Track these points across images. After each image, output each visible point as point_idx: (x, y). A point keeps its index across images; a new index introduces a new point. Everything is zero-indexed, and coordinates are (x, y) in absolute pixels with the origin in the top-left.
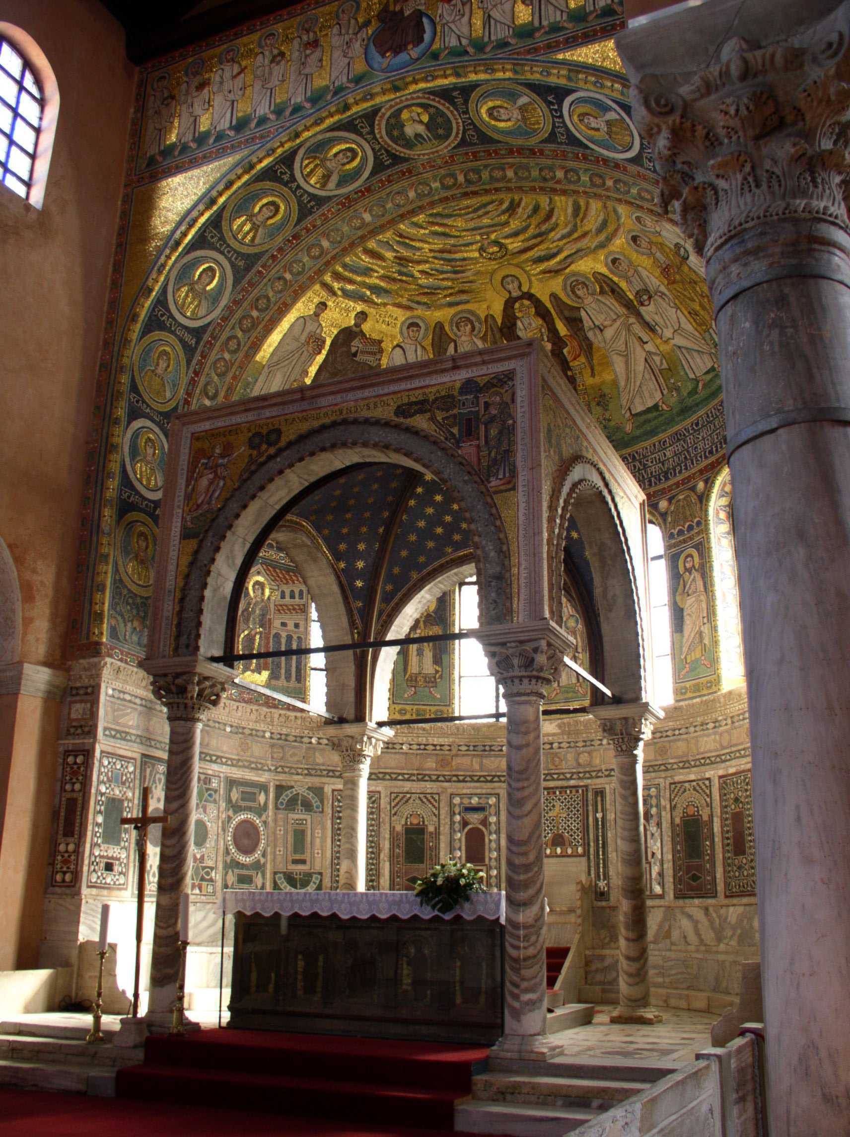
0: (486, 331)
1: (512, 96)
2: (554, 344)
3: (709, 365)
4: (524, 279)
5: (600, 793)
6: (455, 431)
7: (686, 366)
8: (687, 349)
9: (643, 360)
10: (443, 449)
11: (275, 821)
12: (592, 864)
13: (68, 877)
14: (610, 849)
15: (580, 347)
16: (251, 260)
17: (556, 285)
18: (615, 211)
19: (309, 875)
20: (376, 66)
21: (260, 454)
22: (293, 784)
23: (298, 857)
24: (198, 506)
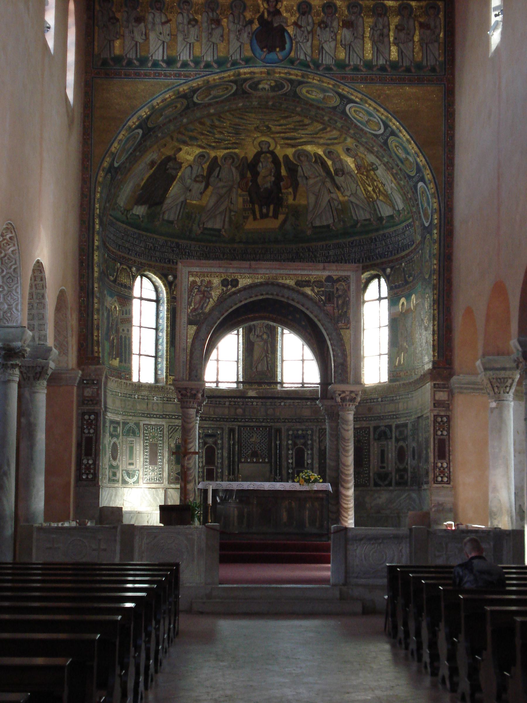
0: (239, 165)
3: (368, 217)
5: (278, 431)
6: (323, 298)
7: (353, 212)
8: (357, 205)
9: (327, 200)
10: (319, 307)
11: (122, 441)
12: (273, 467)
13: (90, 476)
14: (283, 460)
16: (150, 130)
17: (290, 152)
18: (345, 139)
19: (134, 471)
20: (257, 55)
21: (227, 290)
22: (128, 421)
23: (131, 461)
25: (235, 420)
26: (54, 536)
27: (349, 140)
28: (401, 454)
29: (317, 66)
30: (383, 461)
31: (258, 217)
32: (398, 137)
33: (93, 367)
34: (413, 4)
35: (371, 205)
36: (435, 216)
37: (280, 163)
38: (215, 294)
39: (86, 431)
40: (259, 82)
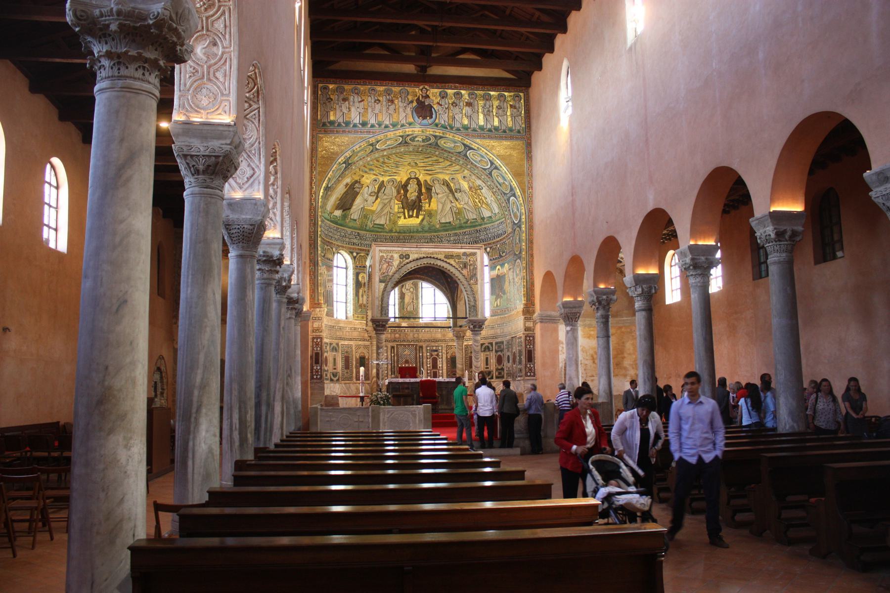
1: (456, 143)
2: (419, 194)
3: (475, 217)
4: (418, 173)
5: (421, 347)
8: (468, 210)
15: (428, 197)
16: (349, 164)
17: (428, 178)
18: (464, 171)
19: (337, 373)
24: (384, 273)
25: (395, 341)
26: (331, 413)
27: (466, 171)
28: (499, 360)
29: (452, 128)
30: (487, 364)
31: (407, 217)
32: (499, 170)
33: (318, 309)
34: (506, 94)
35: (477, 210)
36: (523, 217)
37: (421, 184)
38: (396, 263)
39: (315, 349)
40: (416, 137)
